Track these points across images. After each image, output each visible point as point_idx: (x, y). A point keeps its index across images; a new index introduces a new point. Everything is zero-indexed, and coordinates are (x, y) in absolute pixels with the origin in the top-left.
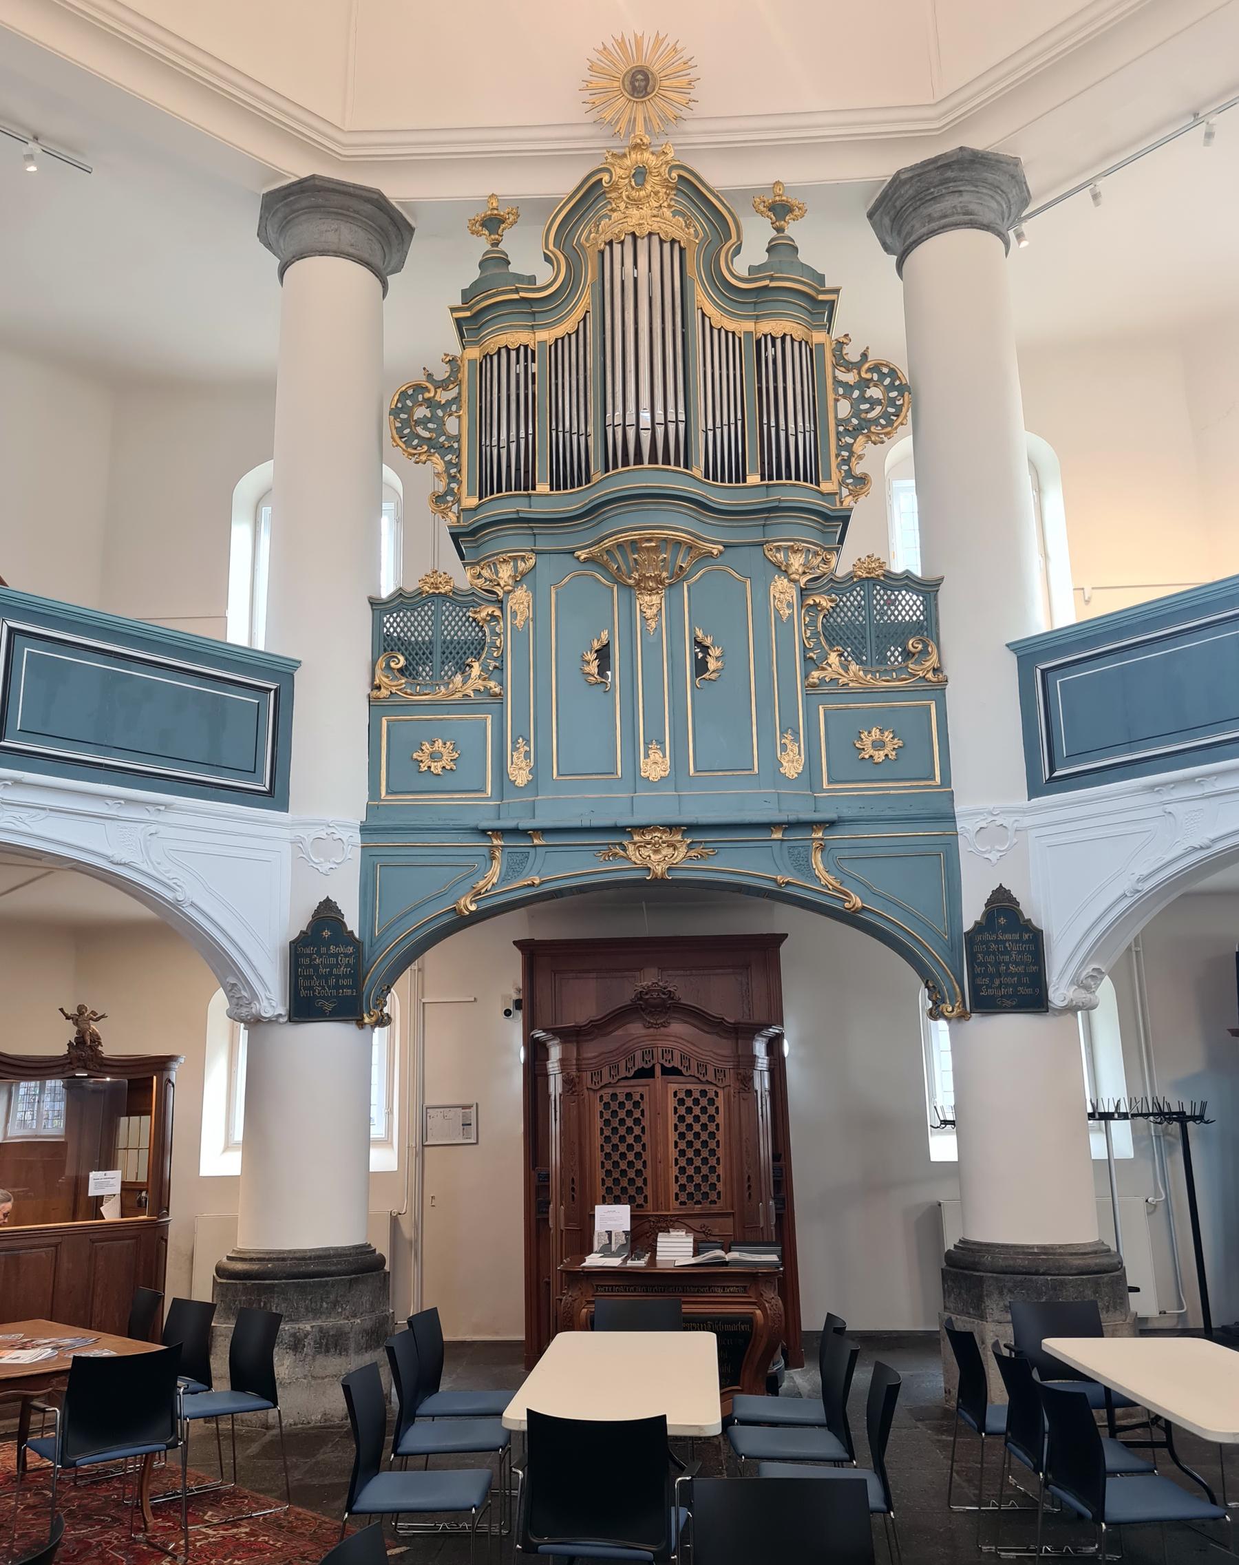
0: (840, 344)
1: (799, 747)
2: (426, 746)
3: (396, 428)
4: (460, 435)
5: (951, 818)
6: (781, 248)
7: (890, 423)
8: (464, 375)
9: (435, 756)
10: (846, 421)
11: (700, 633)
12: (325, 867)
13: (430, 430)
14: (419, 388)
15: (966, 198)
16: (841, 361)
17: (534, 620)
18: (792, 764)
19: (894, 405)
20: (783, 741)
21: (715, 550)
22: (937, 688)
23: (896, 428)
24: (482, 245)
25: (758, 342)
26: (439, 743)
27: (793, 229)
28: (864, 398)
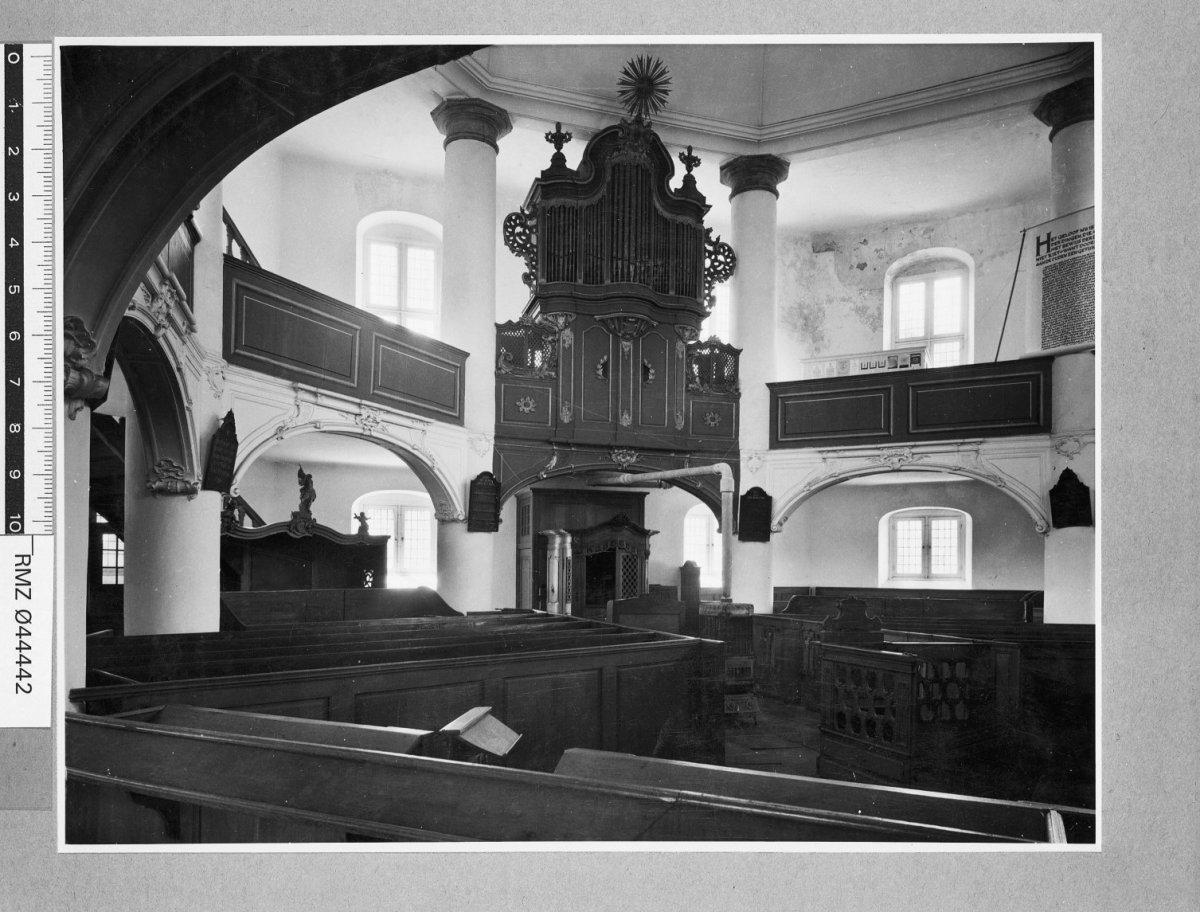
6: (689, 181)
10: (708, 270)
11: (646, 362)
13: (521, 239)
24: (551, 149)
27: (695, 172)
28: (716, 260)
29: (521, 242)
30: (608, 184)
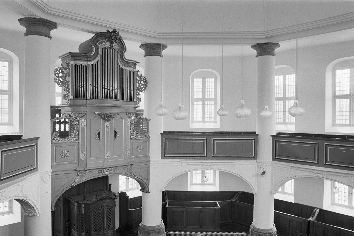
0: (138, 72)
3: (56, 78)
4: (69, 81)
5: (150, 161)
7: (144, 89)
8: (70, 67)
14: (60, 69)
16: (138, 76)
17: (86, 126)
22: (148, 139)
28: (141, 83)
30: (100, 55)
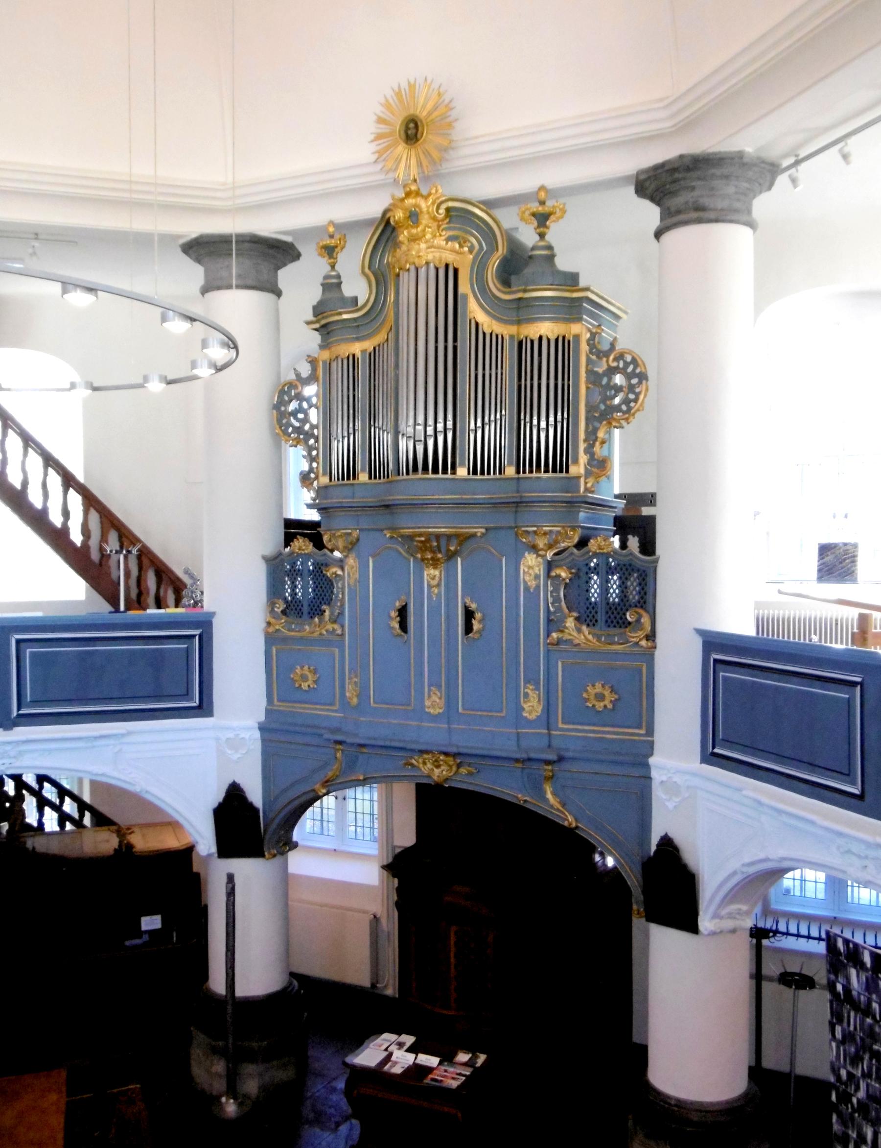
1: (539, 695)
2: (298, 671)
9: (304, 678)
12: (236, 756)
15: (696, 193)
18: (533, 707)
19: (634, 393)
20: (526, 690)
21: (480, 531)
23: (634, 414)
25: (520, 343)
26: (306, 667)
29: (297, 424)
